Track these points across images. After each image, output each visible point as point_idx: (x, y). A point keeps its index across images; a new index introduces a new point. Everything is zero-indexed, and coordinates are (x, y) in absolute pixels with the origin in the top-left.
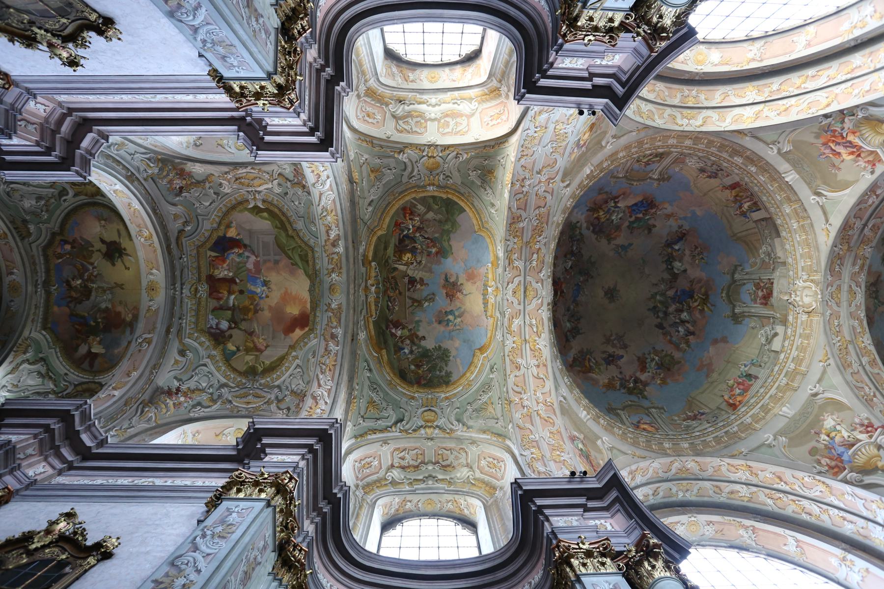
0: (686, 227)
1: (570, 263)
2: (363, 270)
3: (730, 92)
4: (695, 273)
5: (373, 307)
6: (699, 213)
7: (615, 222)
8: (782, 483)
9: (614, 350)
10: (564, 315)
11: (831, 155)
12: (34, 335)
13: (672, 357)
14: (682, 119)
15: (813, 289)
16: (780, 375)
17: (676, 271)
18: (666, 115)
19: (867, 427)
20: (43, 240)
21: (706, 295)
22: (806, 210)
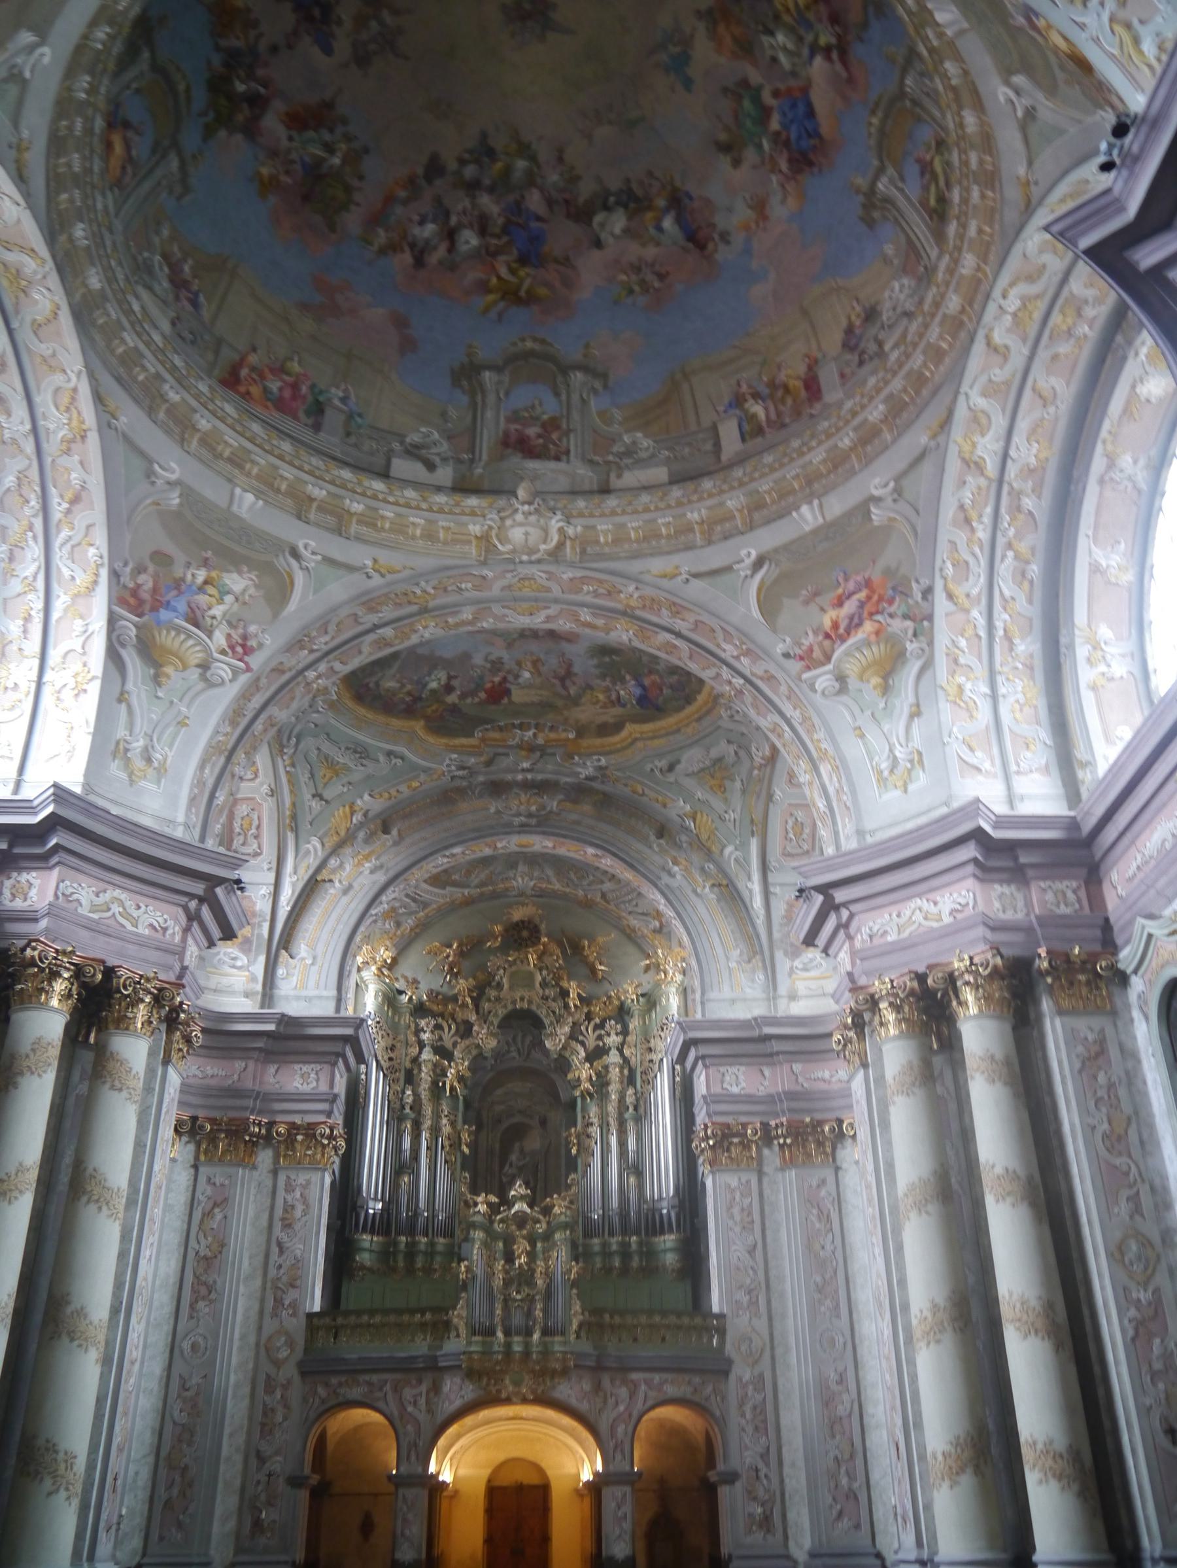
0: (723, 254)
8: (65, 505)
11: (840, 591)
15: (543, 547)
16: (332, 483)
17: (598, 218)
19: (243, 646)
21: (530, 299)
22: (726, 538)
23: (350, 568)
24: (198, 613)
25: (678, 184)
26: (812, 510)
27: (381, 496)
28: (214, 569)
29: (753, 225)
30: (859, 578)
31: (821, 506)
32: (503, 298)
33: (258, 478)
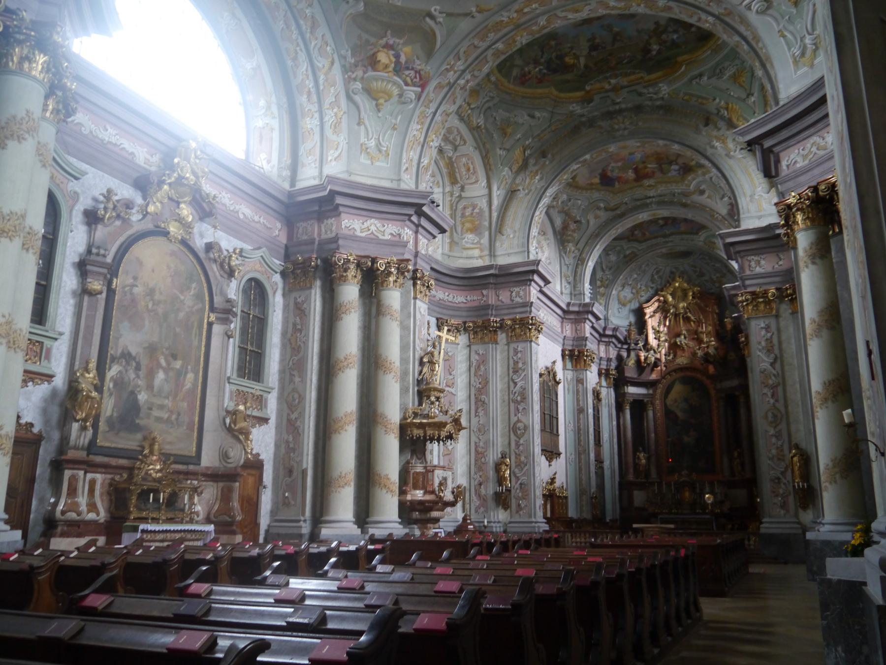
2: (597, 98)
5: (632, 77)
12: (702, 238)
20: (635, 245)
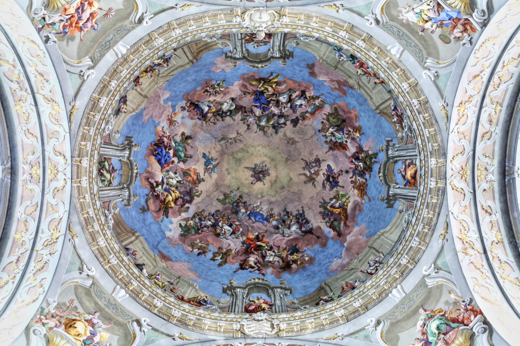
0: (183, 103)
1: (226, 227)
3: (24, 128)
4: (235, 90)
6: (167, 95)
7: (180, 179)
8: (482, 74)
9: (321, 173)
10: (283, 234)
13: (330, 114)
14: (58, 180)
15: (252, 12)
16: (352, 45)
18: (54, 202)
21: (259, 80)
22: (160, 27)
23: (351, 10)
24: (436, 9)
25: (204, 122)
26: (121, 52)
27: (330, 35)
28: (420, 26)
29: (173, 115)
30: (86, 30)
31: (117, 55)
32: (270, 80)
33: (387, 56)
